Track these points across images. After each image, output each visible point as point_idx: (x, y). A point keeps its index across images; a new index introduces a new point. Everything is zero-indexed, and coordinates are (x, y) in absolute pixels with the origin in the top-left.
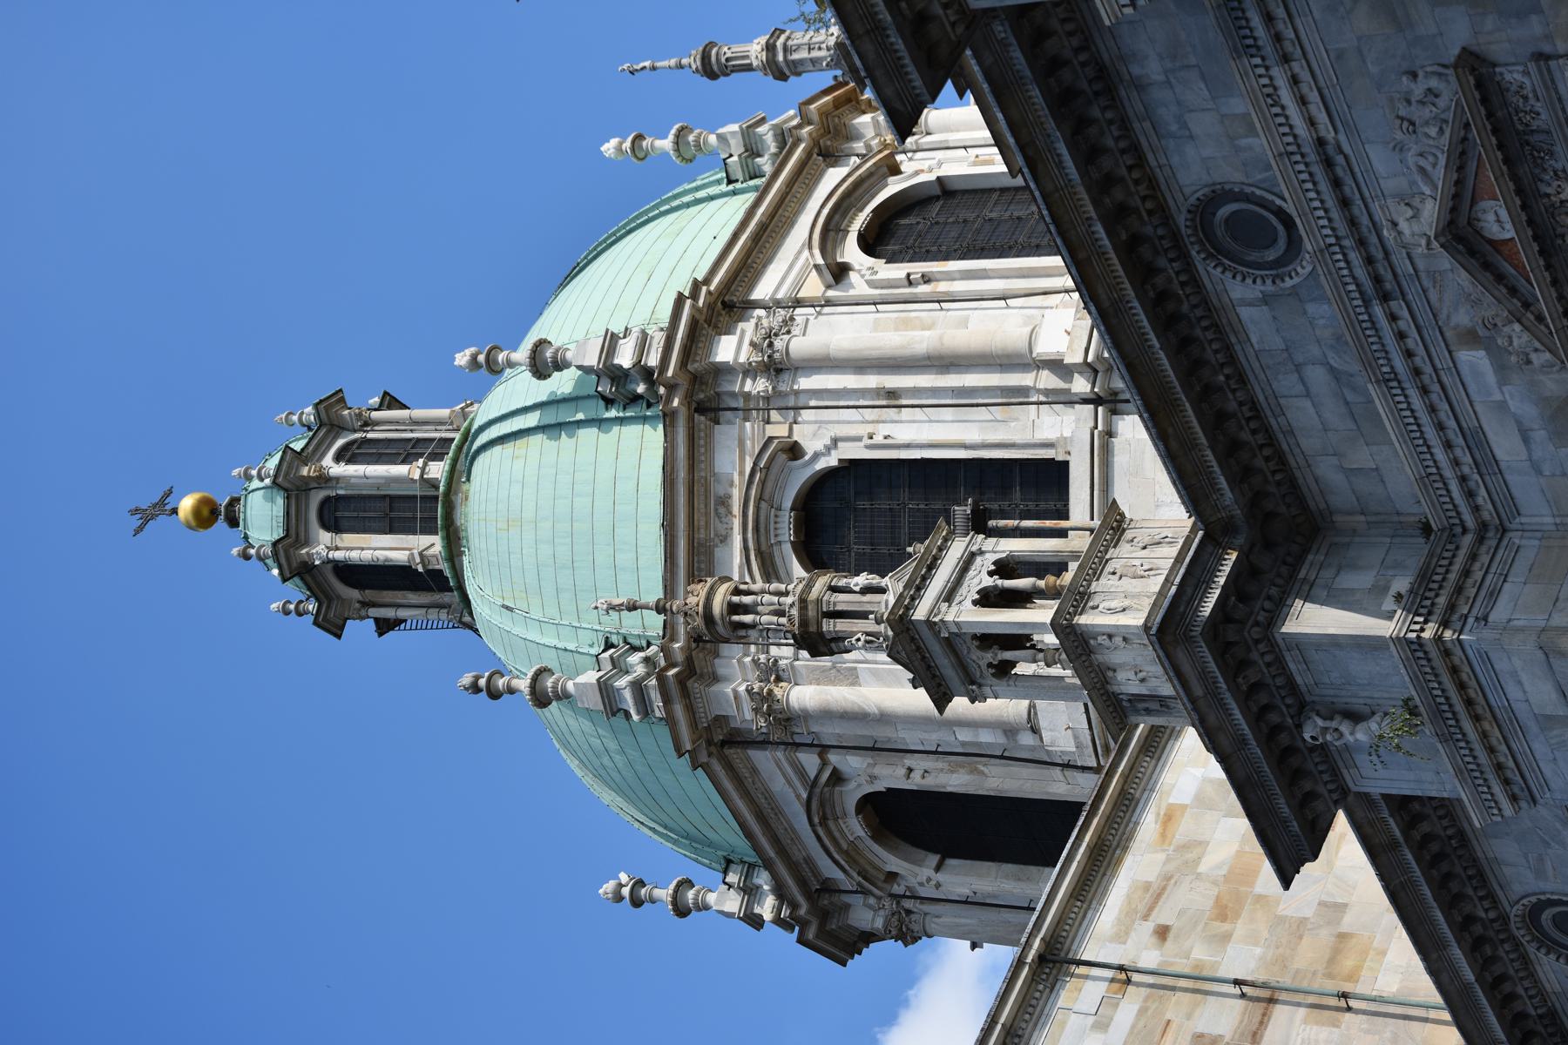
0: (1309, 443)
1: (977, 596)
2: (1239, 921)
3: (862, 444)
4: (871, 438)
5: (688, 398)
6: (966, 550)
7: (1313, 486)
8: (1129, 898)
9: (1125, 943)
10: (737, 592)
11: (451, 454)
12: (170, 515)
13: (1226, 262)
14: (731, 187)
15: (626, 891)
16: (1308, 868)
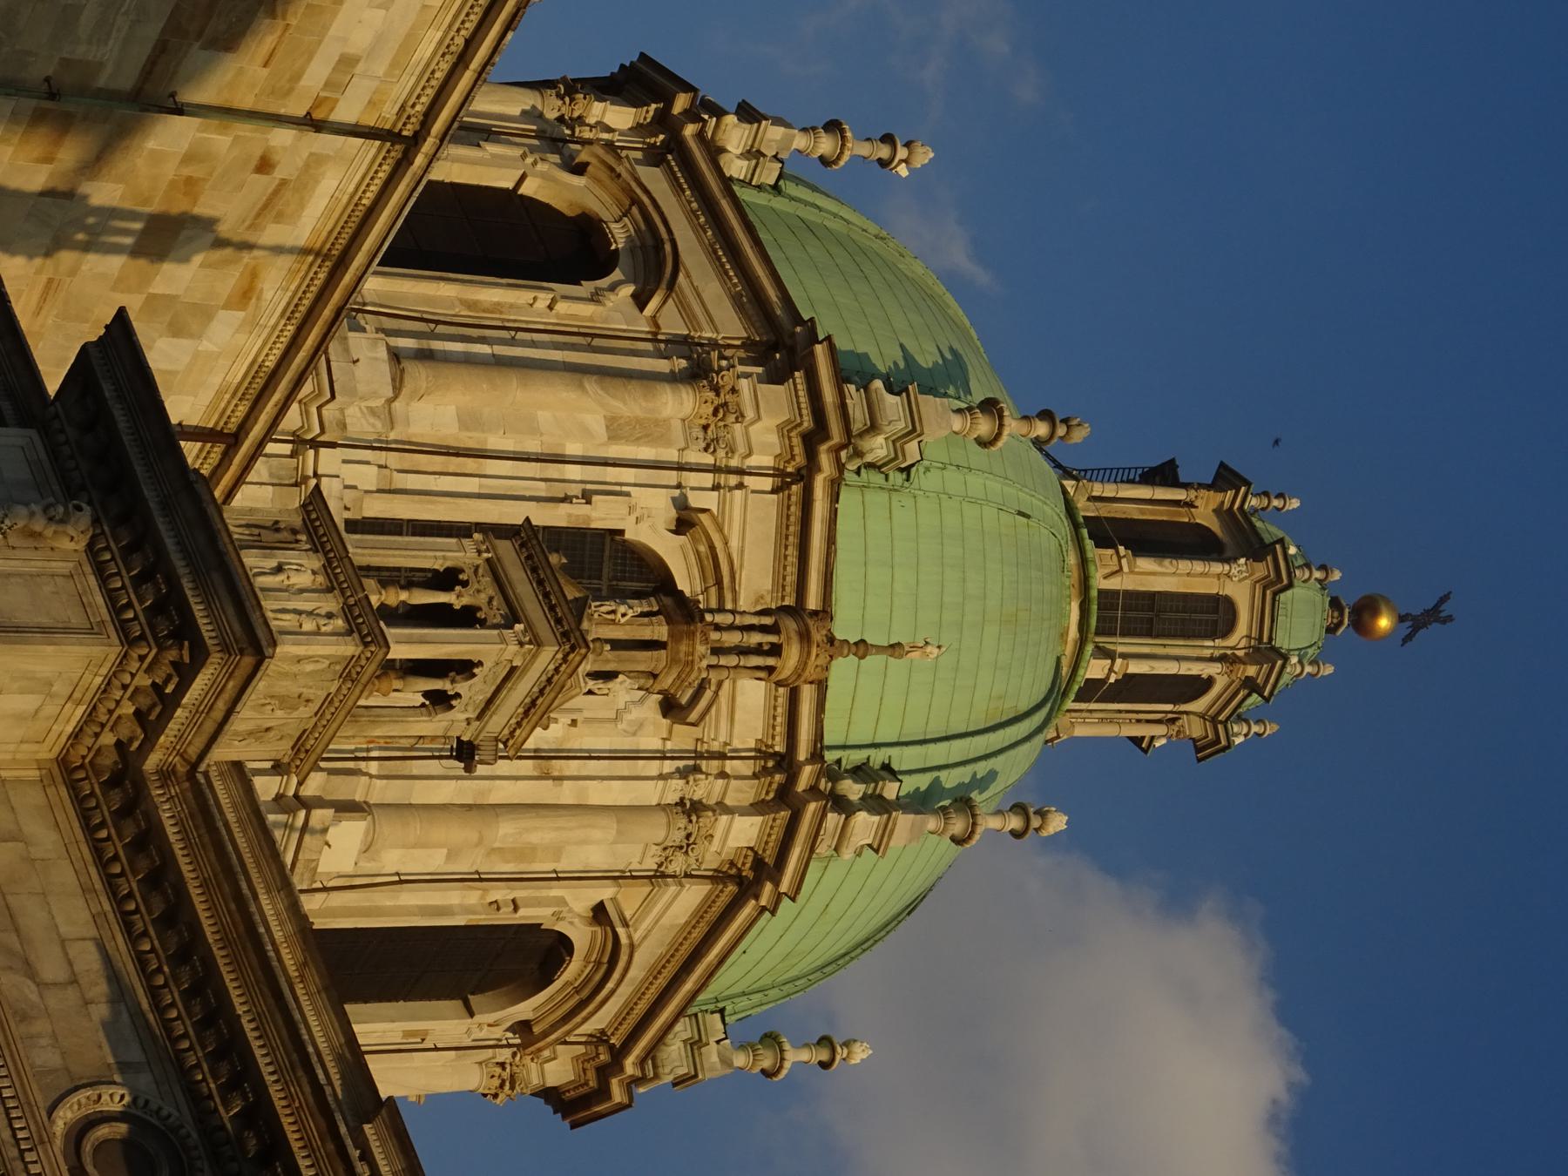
0: (65, 876)
1: (476, 671)
2: (171, 177)
3: (587, 714)
4: (573, 720)
5: (792, 778)
6: (487, 722)
7: (61, 818)
8: (302, 206)
9: (311, 154)
10: (770, 670)
11: (1076, 687)
12: (1407, 614)
13: (154, 1121)
14: (720, 1005)
15: (902, 153)
16: (94, 333)
